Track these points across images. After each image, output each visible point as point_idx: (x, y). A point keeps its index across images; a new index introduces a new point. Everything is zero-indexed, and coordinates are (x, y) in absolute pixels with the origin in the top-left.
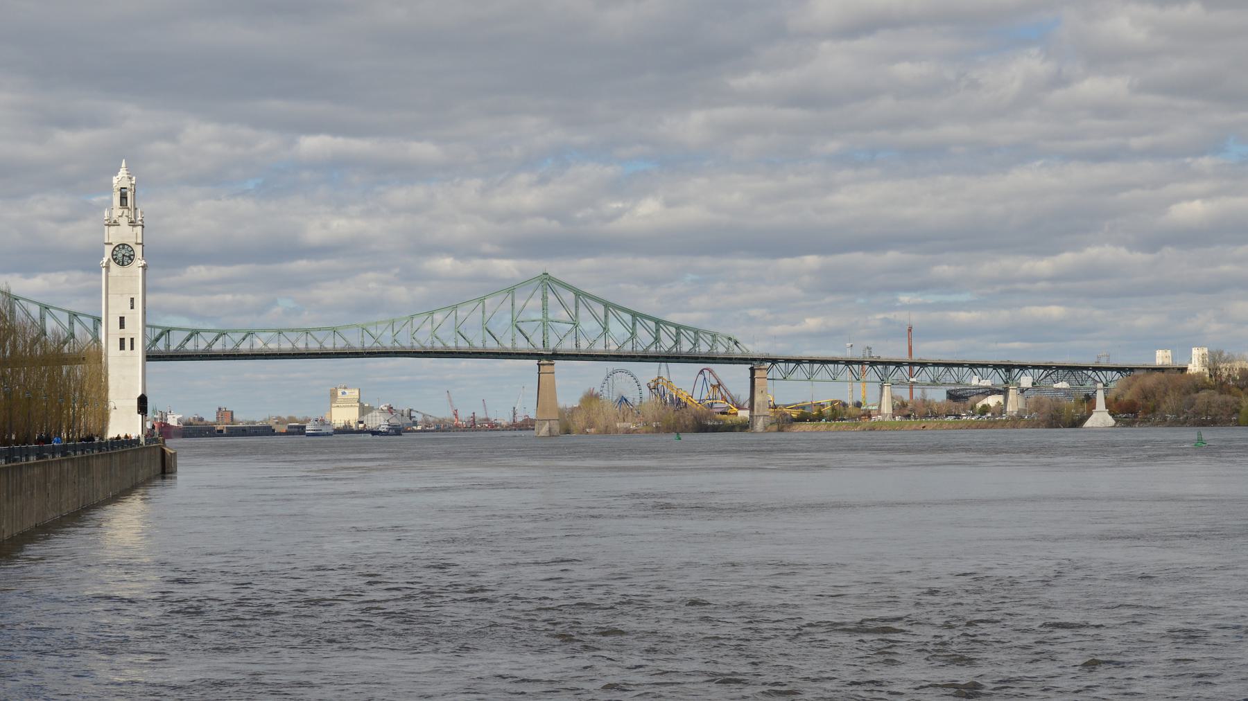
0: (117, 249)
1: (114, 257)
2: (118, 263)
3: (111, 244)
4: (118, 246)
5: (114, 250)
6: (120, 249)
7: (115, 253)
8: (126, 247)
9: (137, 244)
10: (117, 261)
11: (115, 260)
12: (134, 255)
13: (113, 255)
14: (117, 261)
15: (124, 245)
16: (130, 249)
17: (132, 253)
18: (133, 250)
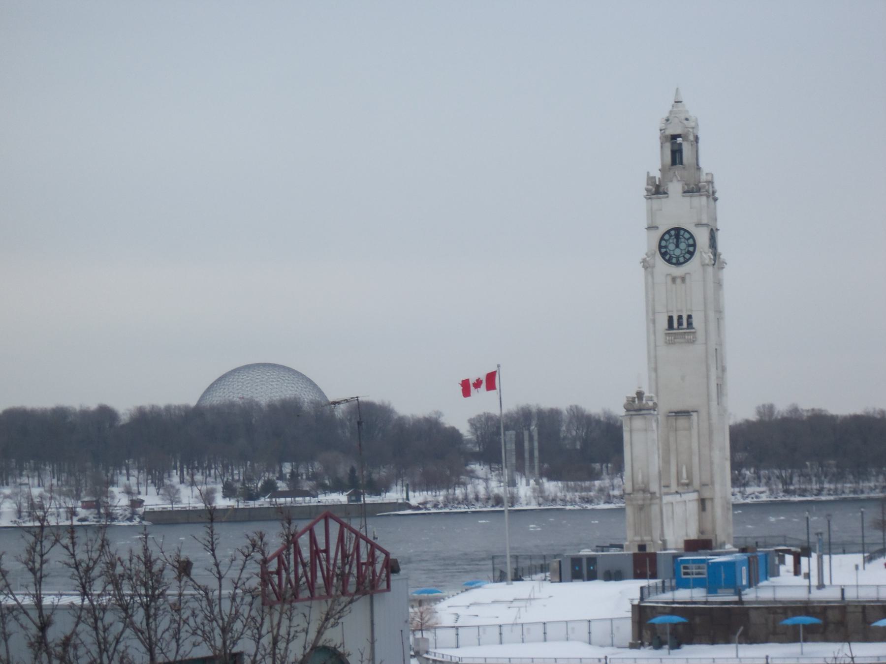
0: (667, 237)
1: (663, 250)
2: (669, 261)
3: (657, 228)
4: (668, 232)
5: (662, 239)
7: (663, 243)
9: (699, 225)
10: (667, 257)
11: (663, 255)
12: (694, 245)
13: (660, 247)
14: (667, 257)
15: (678, 230)
17: (691, 242)
18: (692, 237)
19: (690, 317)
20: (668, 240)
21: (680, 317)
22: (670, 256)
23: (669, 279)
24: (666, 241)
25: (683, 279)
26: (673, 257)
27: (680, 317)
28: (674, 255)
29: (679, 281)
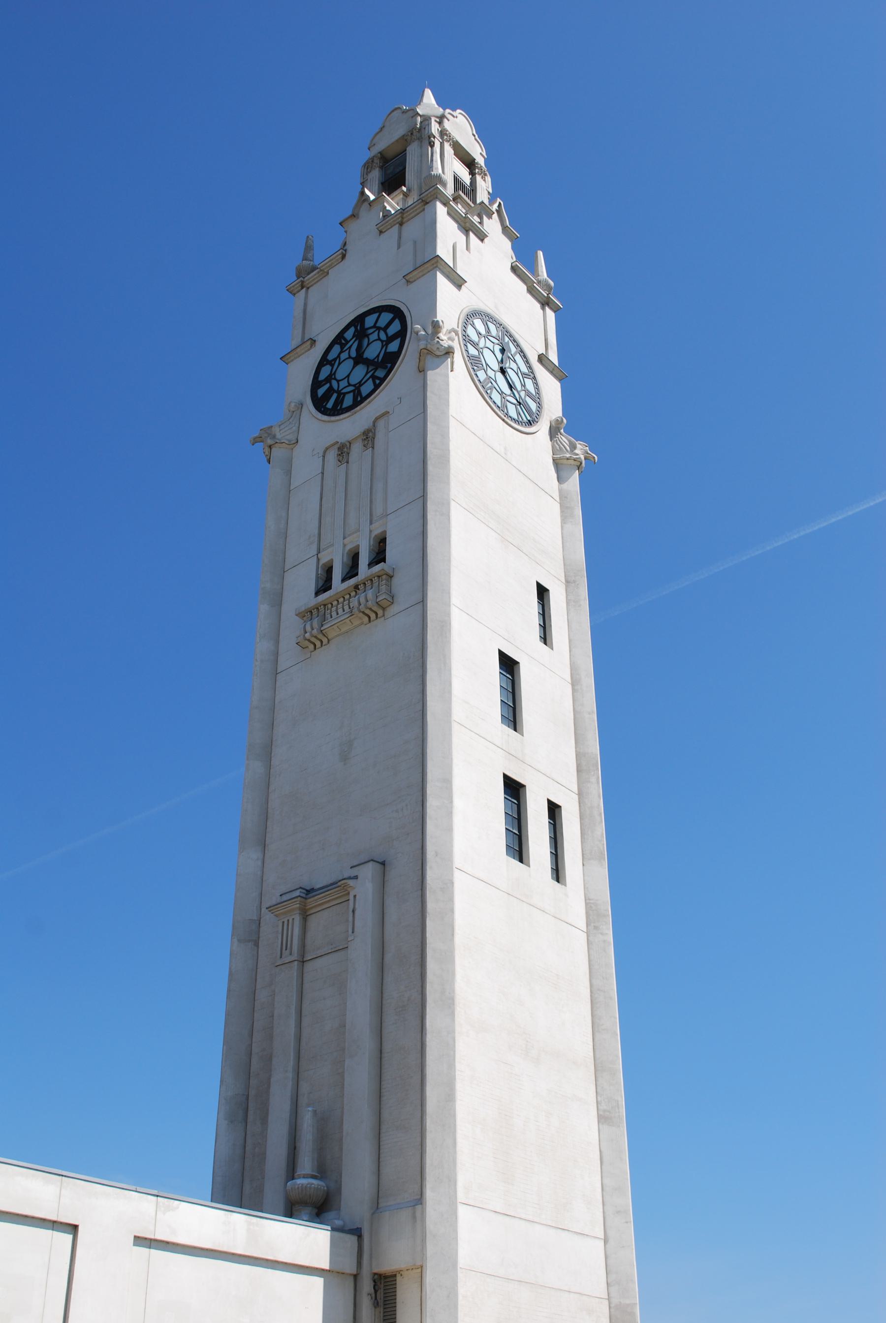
1: (321, 392)
4: (339, 339)
5: (324, 361)
6: (342, 346)
8: (370, 321)
10: (330, 405)
14: (330, 405)
15: (360, 320)
16: (386, 317)
19: (382, 542)
20: (335, 360)
21: (355, 558)
22: (339, 392)
23: (332, 455)
24: (331, 363)
25: (368, 437)
26: (345, 394)
27: (355, 558)
28: (349, 385)
29: (356, 449)
